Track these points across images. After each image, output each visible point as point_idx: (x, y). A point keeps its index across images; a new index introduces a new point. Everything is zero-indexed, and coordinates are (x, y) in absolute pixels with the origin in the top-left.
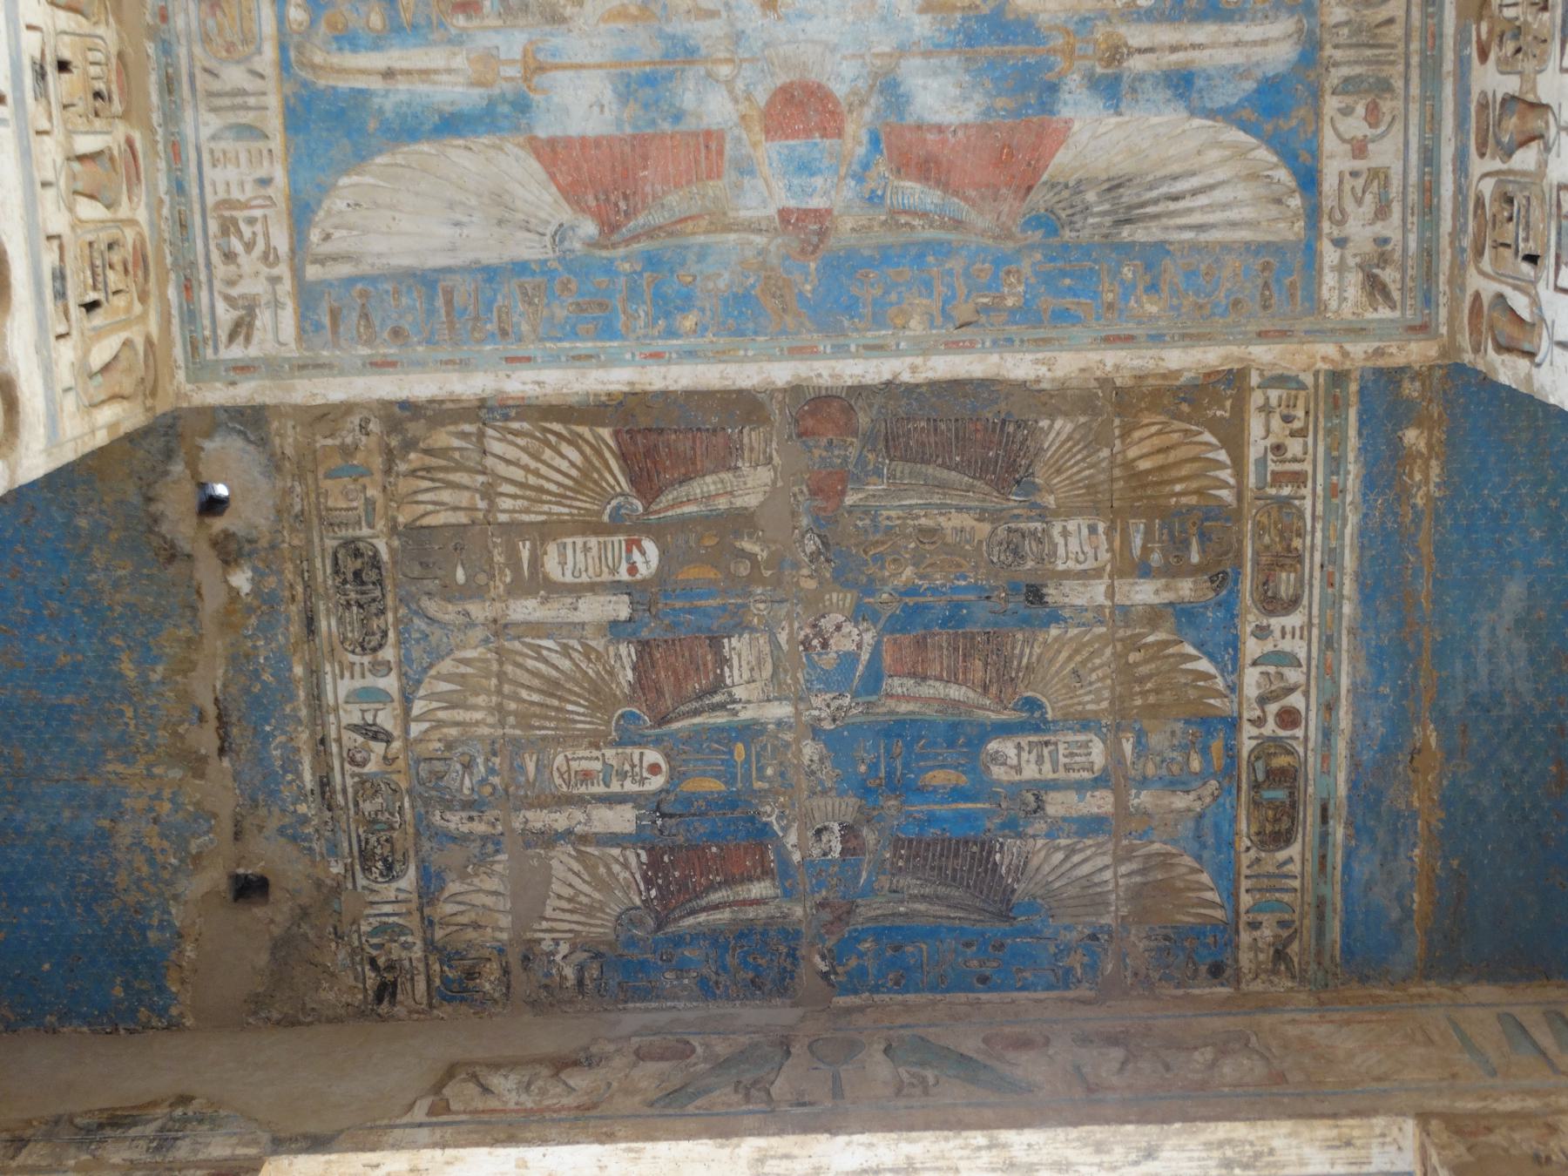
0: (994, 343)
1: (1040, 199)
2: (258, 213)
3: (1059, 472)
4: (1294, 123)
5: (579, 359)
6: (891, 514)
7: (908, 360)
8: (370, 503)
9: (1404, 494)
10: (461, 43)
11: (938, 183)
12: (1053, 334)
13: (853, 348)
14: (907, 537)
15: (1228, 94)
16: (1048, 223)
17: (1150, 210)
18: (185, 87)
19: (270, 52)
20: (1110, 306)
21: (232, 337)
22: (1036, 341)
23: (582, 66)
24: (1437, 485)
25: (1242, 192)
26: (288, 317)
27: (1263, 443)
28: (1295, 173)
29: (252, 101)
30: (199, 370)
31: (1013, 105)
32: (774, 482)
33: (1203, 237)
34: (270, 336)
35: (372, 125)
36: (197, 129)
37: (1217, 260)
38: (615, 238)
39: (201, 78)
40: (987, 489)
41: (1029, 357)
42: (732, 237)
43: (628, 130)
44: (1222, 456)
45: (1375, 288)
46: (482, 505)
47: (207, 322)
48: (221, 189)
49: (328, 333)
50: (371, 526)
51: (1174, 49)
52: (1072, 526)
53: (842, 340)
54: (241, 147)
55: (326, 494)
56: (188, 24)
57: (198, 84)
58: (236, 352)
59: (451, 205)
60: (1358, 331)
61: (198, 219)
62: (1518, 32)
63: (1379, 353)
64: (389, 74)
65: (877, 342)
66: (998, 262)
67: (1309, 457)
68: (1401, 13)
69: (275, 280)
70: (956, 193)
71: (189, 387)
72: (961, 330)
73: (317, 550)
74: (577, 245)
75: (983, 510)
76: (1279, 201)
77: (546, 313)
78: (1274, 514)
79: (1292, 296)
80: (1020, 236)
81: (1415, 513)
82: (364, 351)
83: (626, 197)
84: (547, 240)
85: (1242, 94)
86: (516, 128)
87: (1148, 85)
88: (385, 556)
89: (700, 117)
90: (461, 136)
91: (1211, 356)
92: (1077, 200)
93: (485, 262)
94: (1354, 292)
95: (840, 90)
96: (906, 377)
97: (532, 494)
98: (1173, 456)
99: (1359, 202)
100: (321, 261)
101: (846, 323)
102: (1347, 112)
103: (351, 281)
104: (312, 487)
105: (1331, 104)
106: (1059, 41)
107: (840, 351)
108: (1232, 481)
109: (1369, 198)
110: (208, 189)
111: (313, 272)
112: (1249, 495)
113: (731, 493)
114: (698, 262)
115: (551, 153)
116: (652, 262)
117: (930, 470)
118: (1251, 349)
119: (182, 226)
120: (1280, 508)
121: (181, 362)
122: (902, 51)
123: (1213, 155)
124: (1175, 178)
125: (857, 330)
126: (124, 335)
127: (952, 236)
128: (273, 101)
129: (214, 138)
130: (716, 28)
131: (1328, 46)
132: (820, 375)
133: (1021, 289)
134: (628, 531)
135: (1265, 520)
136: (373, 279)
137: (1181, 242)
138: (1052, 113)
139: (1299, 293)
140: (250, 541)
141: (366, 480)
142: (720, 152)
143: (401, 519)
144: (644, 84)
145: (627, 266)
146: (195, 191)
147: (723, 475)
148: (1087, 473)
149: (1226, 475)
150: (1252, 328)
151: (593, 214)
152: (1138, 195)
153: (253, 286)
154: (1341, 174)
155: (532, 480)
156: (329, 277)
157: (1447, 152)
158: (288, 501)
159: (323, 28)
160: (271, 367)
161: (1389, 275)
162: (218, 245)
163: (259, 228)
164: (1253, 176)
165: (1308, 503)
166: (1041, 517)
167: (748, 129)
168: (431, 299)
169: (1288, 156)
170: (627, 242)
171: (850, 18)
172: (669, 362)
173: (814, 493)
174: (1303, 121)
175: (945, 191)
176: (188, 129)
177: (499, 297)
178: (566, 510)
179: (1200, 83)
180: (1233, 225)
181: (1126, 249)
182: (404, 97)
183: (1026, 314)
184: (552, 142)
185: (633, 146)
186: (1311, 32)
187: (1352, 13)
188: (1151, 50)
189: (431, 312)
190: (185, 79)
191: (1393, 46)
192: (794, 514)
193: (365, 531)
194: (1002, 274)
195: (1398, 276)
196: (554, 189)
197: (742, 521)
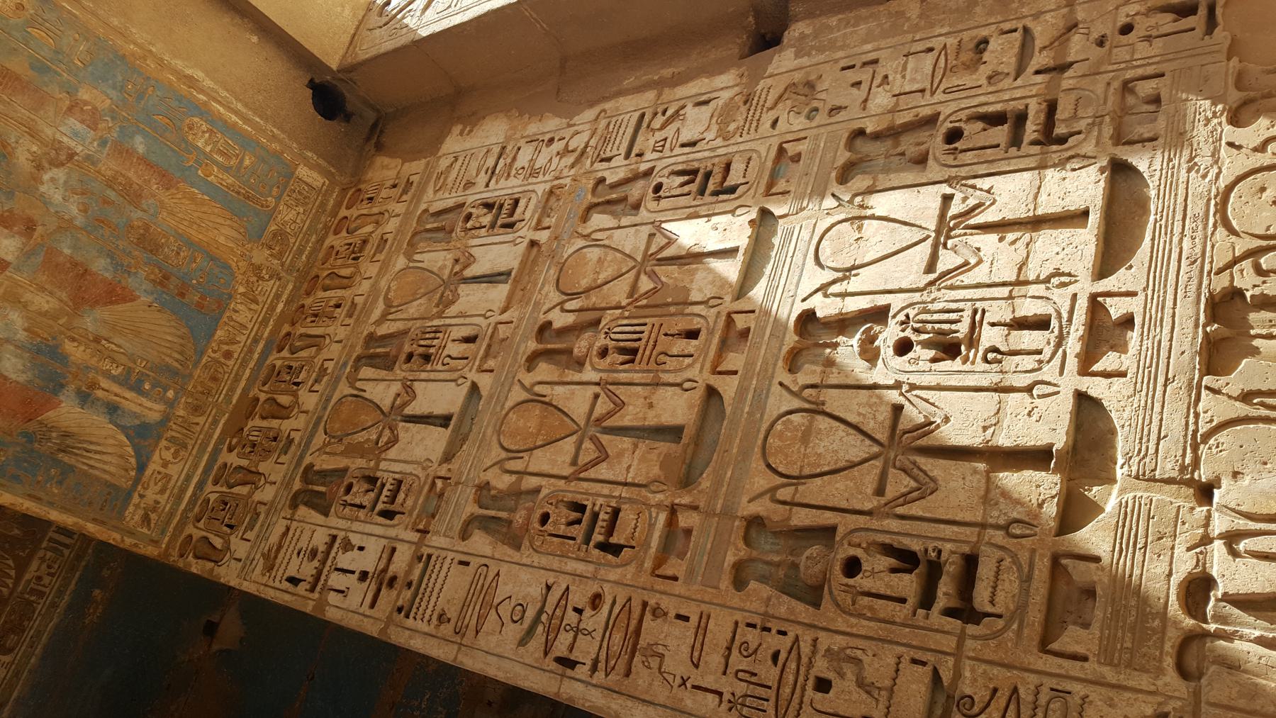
15: (127, 422)
45: (146, 519)
51: (116, 395)
60: (131, 533)
94: (137, 518)
102: (168, 448)
105: (164, 443)
123: (111, 441)
161: (153, 516)
164: (121, 456)
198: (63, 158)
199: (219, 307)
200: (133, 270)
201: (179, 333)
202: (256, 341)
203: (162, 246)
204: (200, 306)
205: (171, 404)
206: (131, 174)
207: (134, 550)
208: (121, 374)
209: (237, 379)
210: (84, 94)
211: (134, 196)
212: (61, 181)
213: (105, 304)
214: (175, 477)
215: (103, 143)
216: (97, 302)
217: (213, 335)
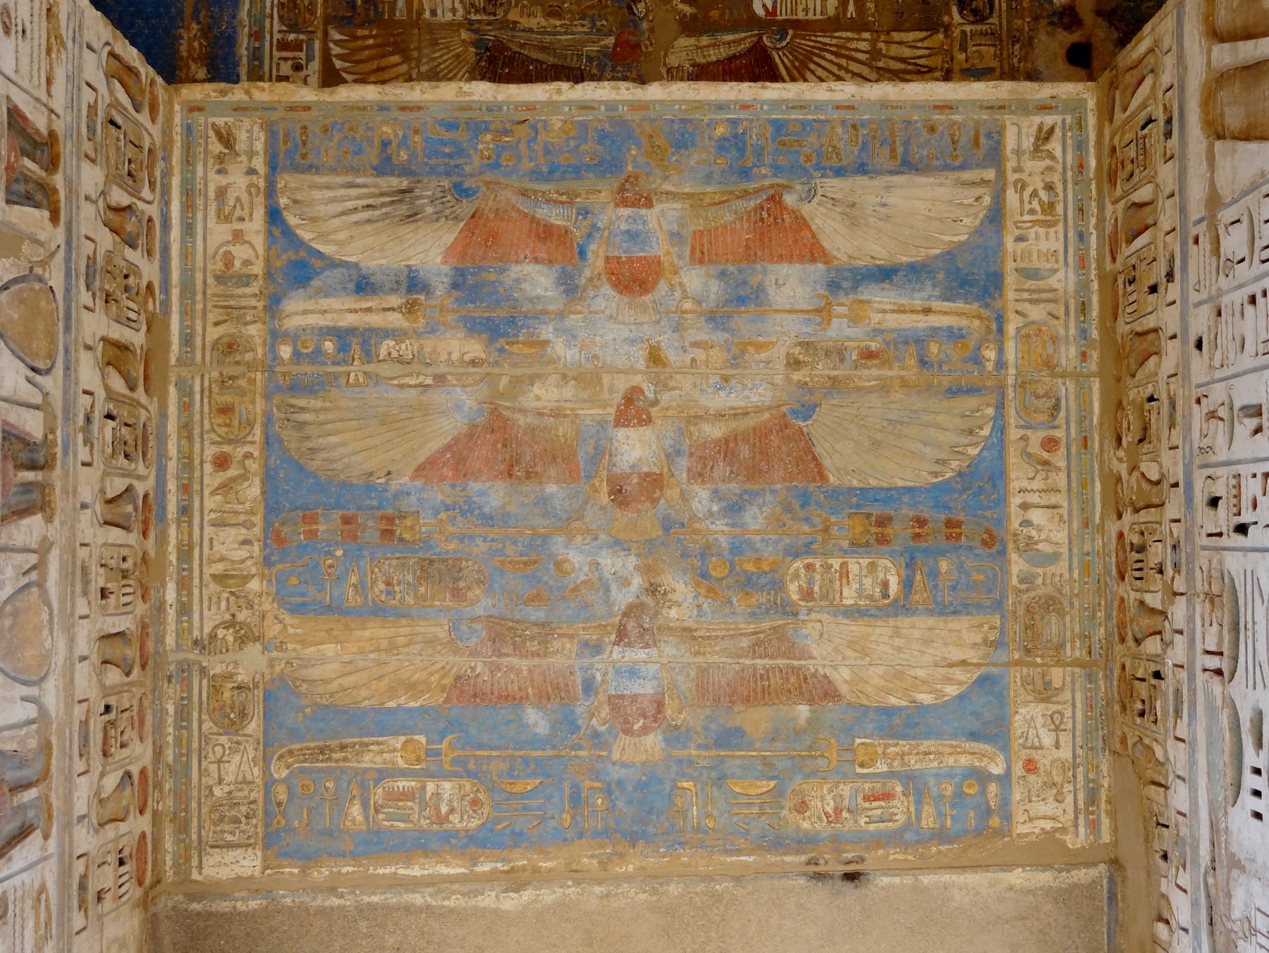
0: (500, 109)
1: (466, 208)
2: (1027, 217)
3: (458, 56)
4: (285, 256)
5: (802, 106)
6: (582, 28)
7: (562, 98)
8: (963, 48)
9: (206, 31)
10: (875, 330)
11: (538, 223)
12: (457, 114)
13: (603, 108)
14: (570, 11)
15: (332, 277)
16: (461, 191)
17: (389, 199)
18: (1072, 308)
19: (1011, 329)
20: (416, 132)
21: (1051, 131)
22: (471, 109)
23: (789, 312)
24: (181, 37)
25: (322, 210)
26: (1010, 143)
27: (309, 72)
28: (284, 222)
29: (1026, 295)
30: (1077, 107)
31: (484, 275)
32: (666, 55)
33: (349, 179)
34: (1024, 130)
35: (941, 276)
36: (1066, 278)
37: (339, 161)
38: (771, 192)
39: (1061, 312)
40: (510, 45)
41: (475, 98)
42: (687, 190)
43: (758, 267)
44: (338, 64)
45: (226, 139)
46: (881, 45)
47: (1069, 142)
48: (1052, 235)
49: (982, 132)
50: (964, 32)
51: (369, 310)
52: (449, 16)
53: (611, 114)
54: (1035, 264)
55: (995, 55)
56: (1067, 350)
57: (1063, 309)
58: (1049, 120)
59: (888, 218)
61: (1070, 214)
62: (127, 289)
63: (223, 93)
64: (927, 311)
65: (584, 112)
66: (497, 166)
67: (275, 60)
68: (210, 329)
69: (1018, 169)
70: (526, 215)
71: (1085, 96)
72: (525, 118)
73: (1004, 15)
74: (799, 187)
75: (513, 29)
76: (295, 202)
77: (823, 140)
78: (300, 20)
79: (286, 135)
80: (481, 184)
81: (198, 18)
82: (956, 117)
83: (762, 220)
84: (820, 192)
85: (322, 277)
86: (837, 270)
87: (388, 286)
88: (954, 9)
89: (707, 274)
90: (878, 266)
91: (346, 94)
92: (439, 207)
93: (865, 178)
94: (242, 137)
95: (607, 289)
96: (565, 86)
97: (844, 52)
98: (374, 65)
99: (238, 199)
100: (984, 182)
101: (607, 126)
102: (247, 263)
103: (962, 167)
104: (1005, 62)
105: (258, 268)
106: (450, 318)
107: (612, 106)
108: (331, 45)
109: (231, 203)
110: (1061, 235)
111: (990, 174)
112: (319, 35)
113: (698, 47)
114: (712, 173)
115: (814, 252)
116: (745, 174)
117: (551, 60)
118: (316, 99)
119: (1081, 210)
120: (296, 24)
121: (1090, 114)
122: (561, 315)
123: (341, 236)
124: (369, 221)
125: (600, 121)
126: (1128, 113)
127: (529, 185)
128: (1010, 295)
129: (1055, 271)
130: (693, 335)
131: (261, 308)
132: (628, 89)
133: (480, 147)
134: (774, 22)
135: (308, 16)
136: (947, 167)
137: (365, 176)
138: (456, 269)
139: (281, 137)
140: (1052, 23)
141: (966, 66)
142: (693, 249)
143: (941, 36)
144: (746, 297)
145: (764, 171)
146: (1071, 234)
147: (704, 61)
148: (437, 55)
149: (336, 50)
150: (314, 113)
151: (786, 209)
152: (396, 210)
153: (1033, 165)
154: (251, 220)
155: (843, 62)
156: (979, 171)
157: (175, 233)
158: (1023, 52)
159: (972, 344)
160: (1024, 108)
161: (217, 147)
162: (1057, 195)
163: (1027, 207)
164: (313, 220)
165: (276, 28)
166: (471, 23)
167: (672, 265)
168: (906, 152)
169: (288, 233)
170: (762, 189)
171: (598, 339)
172: (736, 102)
173: (637, 46)
174: (278, 257)
175: (533, 217)
176: (1072, 277)
177: (856, 153)
178: (819, 39)
179: (351, 286)
180: (328, 187)
181: (405, 172)
182: (917, 295)
183: (478, 129)
184: (813, 260)
185: (755, 255)
186: (273, 318)
187: (243, 330)
188: (385, 310)
189: (906, 143)
190: (1072, 313)
191: (215, 306)
192: (652, 30)
193: (968, 28)
194: (494, 157)
195: (210, 147)
196: (814, 227)
197: (690, 27)
198: (631, 625)
199: (277, 533)
200: (443, 516)
201: (322, 455)
202: (185, 511)
203: (419, 580)
204: (311, 519)
205: (276, 336)
206: (524, 664)
207: (223, 85)
208: (378, 345)
209: (186, 428)
210: (653, 741)
211: (503, 633)
212: (614, 587)
213: (456, 440)
214: (212, 222)
215: (589, 686)
216: (470, 436)
217: (264, 481)
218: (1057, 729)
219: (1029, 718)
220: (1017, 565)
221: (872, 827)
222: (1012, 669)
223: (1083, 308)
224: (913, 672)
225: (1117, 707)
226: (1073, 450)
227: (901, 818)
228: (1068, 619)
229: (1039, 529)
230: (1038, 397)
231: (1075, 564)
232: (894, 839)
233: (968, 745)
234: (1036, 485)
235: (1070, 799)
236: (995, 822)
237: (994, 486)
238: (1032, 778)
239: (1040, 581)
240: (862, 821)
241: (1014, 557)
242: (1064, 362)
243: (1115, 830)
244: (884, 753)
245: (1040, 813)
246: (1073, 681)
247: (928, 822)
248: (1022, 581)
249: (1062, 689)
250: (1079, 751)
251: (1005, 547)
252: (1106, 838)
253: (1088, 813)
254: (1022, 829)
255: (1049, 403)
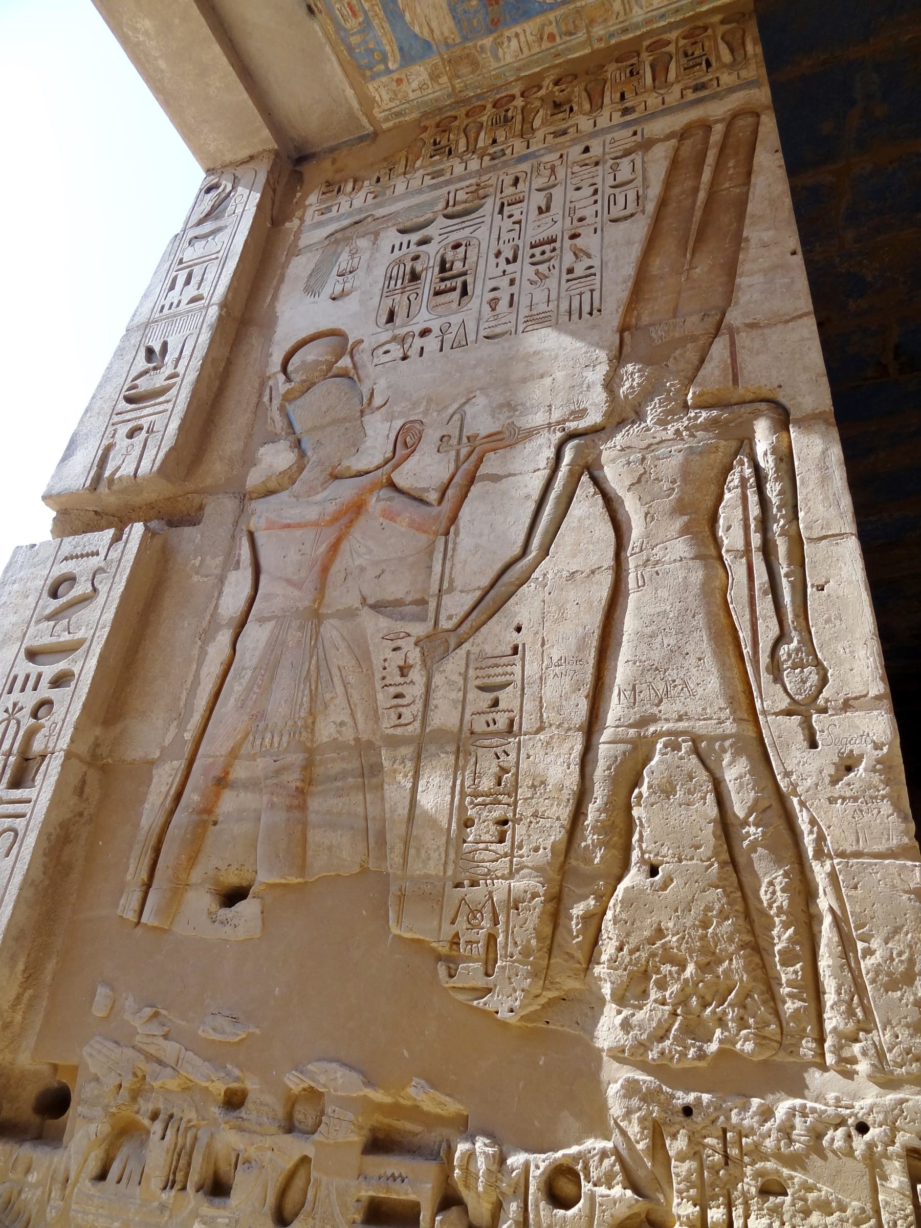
39: (620, 19)
61: (674, 6)
126: (719, 40)
129: (641, 8)
146: (663, 10)
176: (640, 19)
218: (420, 88)
219: (419, 73)
220: (488, 41)
221: (337, 12)
222: (438, 56)
223: (625, 31)
224: (417, 5)
225: (438, 118)
226: (552, 50)
227: (348, 26)
228: (472, 76)
229: (509, 46)
230: (574, 22)
231: (498, 71)
232: (339, 28)
233: (395, 47)
234: (530, 38)
235: (393, 105)
236: (368, 73)
237: (522, 16)
238: (394, 84)
239: (484, 56)
240: (337, 6)
241: (491, 39)
242: (595, 30)
243: (390, 130)
244: (373, 5)
245: (381, 92)
246: (444, 88)
247: (354, 40)
248: (482, 47)
249: (439, 84)
250: (415, 102)
251: (495, 31)
252: (385, 126)
253: (391, 115)
254: (370, 87)
255: (571, 27)
